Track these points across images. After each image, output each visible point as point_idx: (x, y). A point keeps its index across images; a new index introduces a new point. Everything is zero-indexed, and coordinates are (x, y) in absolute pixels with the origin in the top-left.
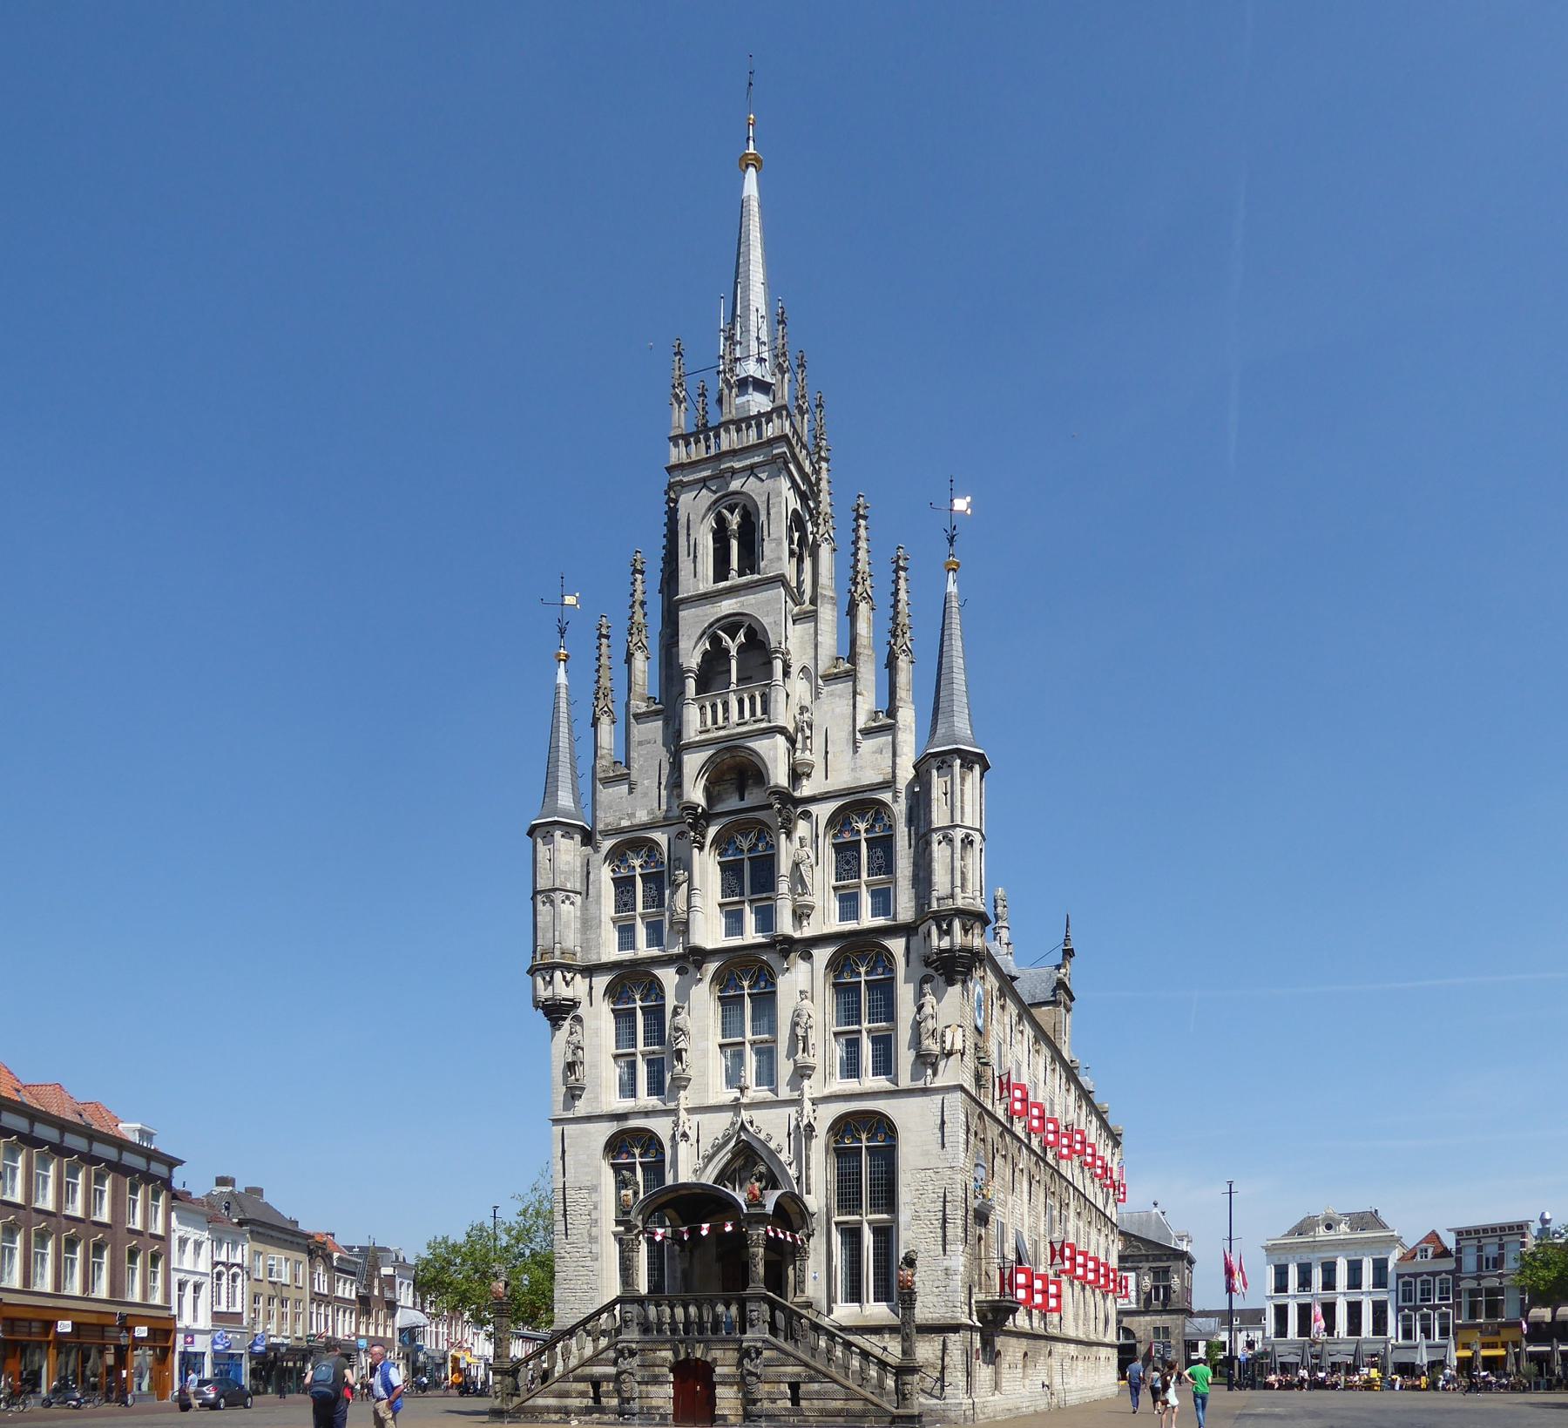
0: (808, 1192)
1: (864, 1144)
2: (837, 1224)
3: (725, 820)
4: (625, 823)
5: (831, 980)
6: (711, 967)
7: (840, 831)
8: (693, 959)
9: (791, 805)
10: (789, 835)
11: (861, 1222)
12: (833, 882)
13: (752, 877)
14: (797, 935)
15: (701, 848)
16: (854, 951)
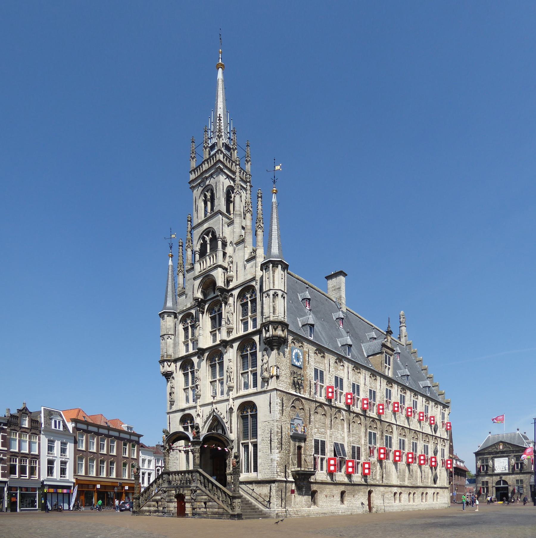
0: (231, 432)
1: (249, 413)
2: (242, 444)
3: (209, 302)
4: (185, 308)
5: (240, 354)
6: (206, 355)
7: (243, 299)
8: (200, 352)
9: (225, 292)
10: (226, 304)
11: (248, 443)
12: (241, 318)
13: (217, 321)
14: (228, 339)
15: (203, 313)
16: (246, 342)
